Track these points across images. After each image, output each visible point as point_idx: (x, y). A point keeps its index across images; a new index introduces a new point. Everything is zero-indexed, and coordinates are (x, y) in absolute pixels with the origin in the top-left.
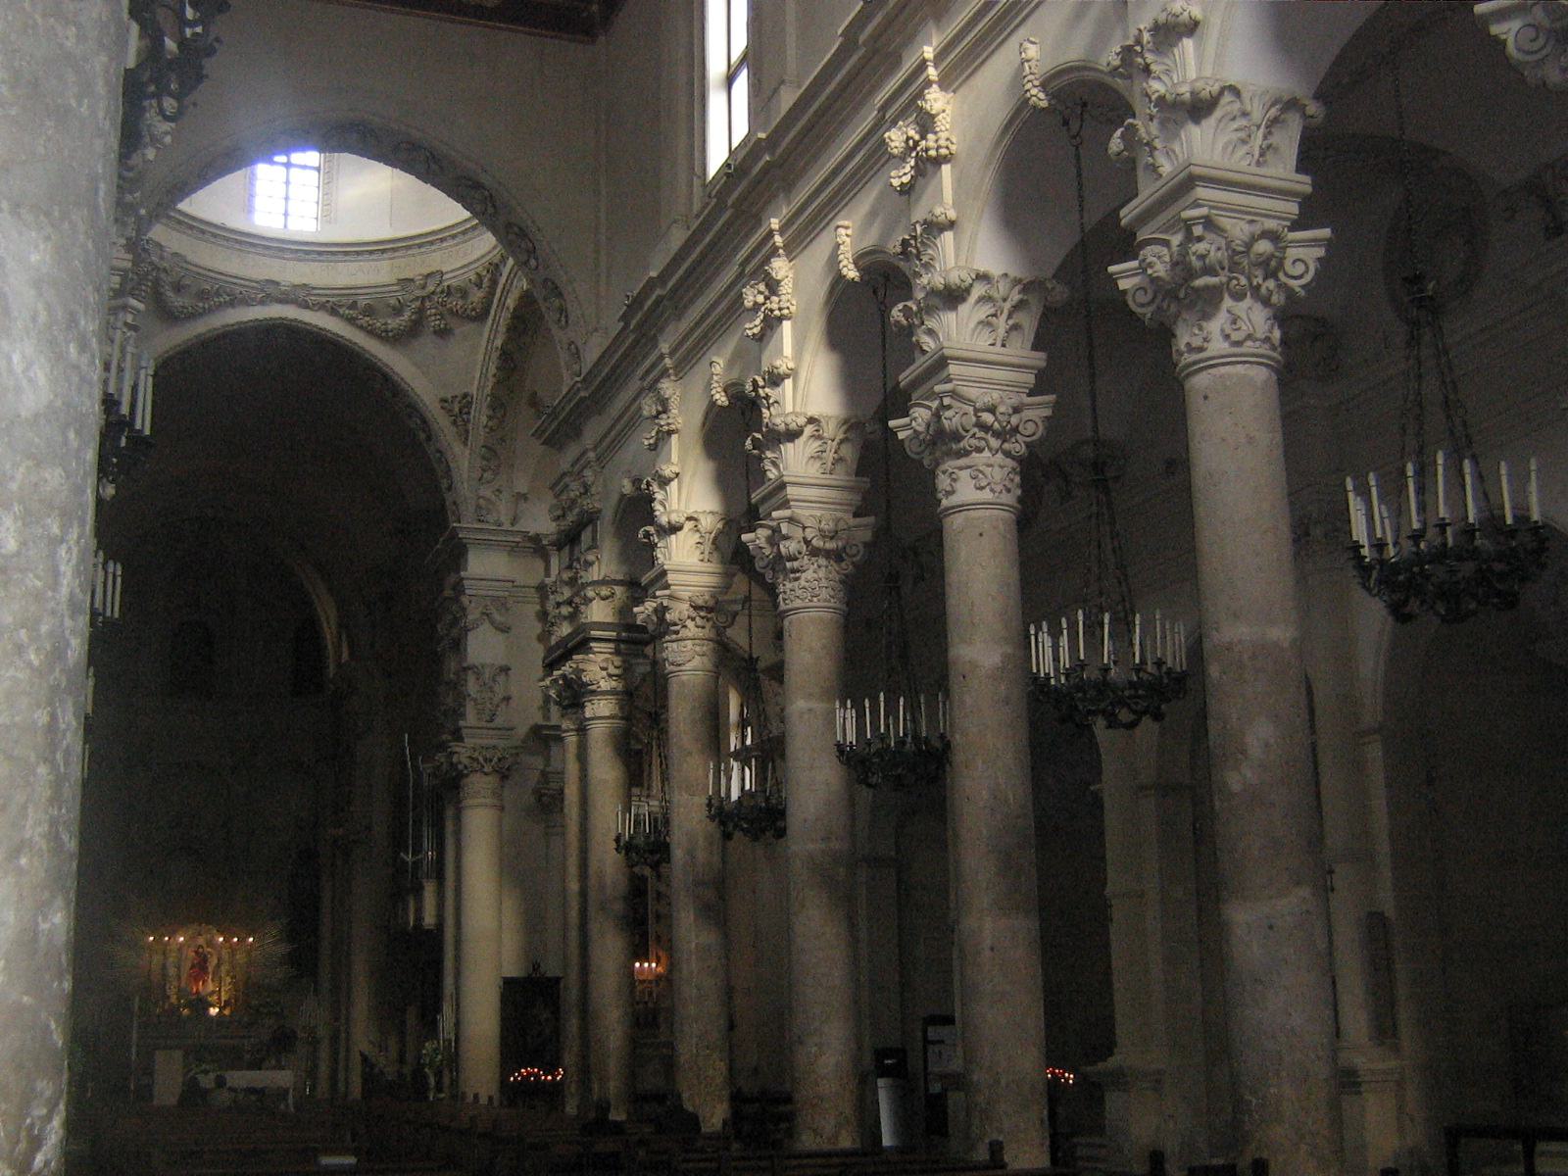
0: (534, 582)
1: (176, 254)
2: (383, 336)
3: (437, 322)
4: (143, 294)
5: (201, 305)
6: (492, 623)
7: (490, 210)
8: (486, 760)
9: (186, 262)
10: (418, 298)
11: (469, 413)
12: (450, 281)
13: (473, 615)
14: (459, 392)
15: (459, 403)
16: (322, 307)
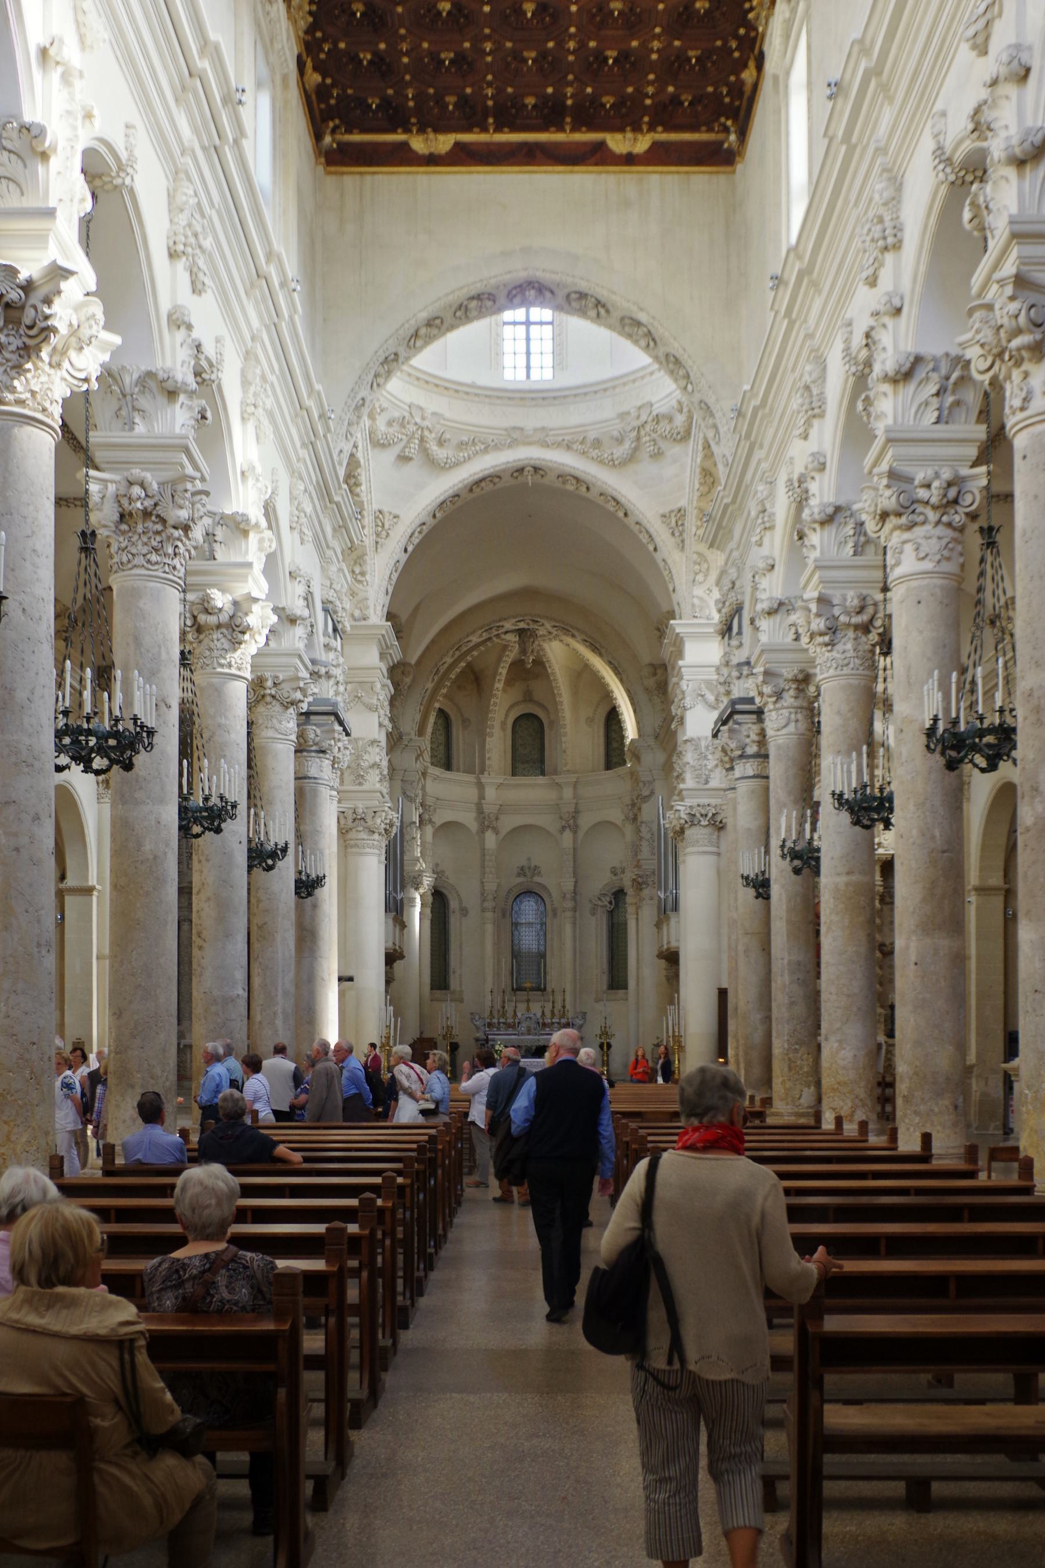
2: (613, 464)
5: (461, 454)
7: (652, 344)
9: (444, 419)
10: (634, 429)
11: (683, 525)
14: (676, 507)
16: (558, 445)
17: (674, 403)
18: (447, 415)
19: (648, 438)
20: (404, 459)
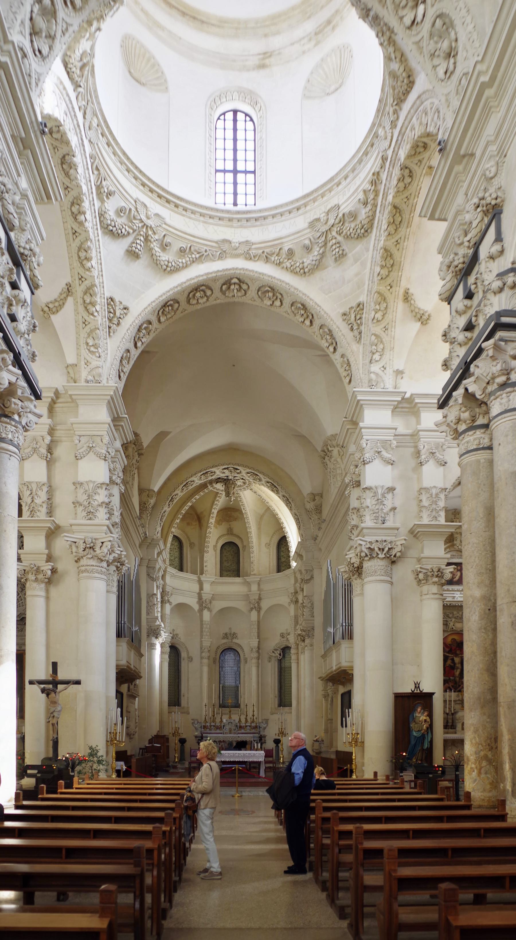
1: (157, 215)
3: (337, 250)
5: (180, 261)
8: (379, 549)
9: (165, 224)
12: (345, 209)
14: (354, 304)
15: (355, 311)
18: (168, 221)
19: (334, 241)
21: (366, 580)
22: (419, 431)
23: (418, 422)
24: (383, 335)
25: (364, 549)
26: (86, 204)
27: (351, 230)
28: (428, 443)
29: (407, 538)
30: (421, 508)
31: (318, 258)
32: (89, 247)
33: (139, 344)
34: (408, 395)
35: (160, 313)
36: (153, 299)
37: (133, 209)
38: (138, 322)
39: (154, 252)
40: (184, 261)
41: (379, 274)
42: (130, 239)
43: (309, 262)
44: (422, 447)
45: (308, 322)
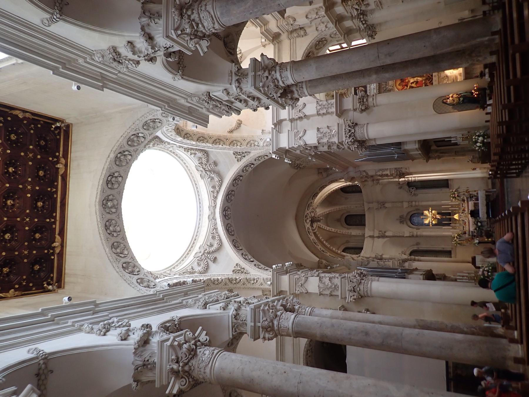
0: (289, 123)
1: (199, 248)
3: (212, 165)
4: (212, 257)
5: (217, 238)
6: (303, 136)
9: (203, 245)
11: (240, 153)
12: (197, 163)
13: (302, 143)
16: (215, 201)
17: (193, 156)
18: (201, 244)
19: (209, 167)
20: (215, 260)
21: (367, 138)
22: (289, 119)
23: (285, 120)
24: (247, 141)
25: (350, 140)
26: (197, 279)
27: (205, 160)
28: (295, 113)
29: (343, 119)
30: (328, 113)
31: (215, 174)
32: (214, 279)
33: (252, 260)
34: (273, 126)
35: (238, 249)
36: (233, 252)
37: (198, 259)
38: (243, 259)
39: (214, 250)
40: (217, 237)
41: (222, 145)
42: (209, 261)
43: (217, 179)
44: (297, 116)
45: (241, 178)
